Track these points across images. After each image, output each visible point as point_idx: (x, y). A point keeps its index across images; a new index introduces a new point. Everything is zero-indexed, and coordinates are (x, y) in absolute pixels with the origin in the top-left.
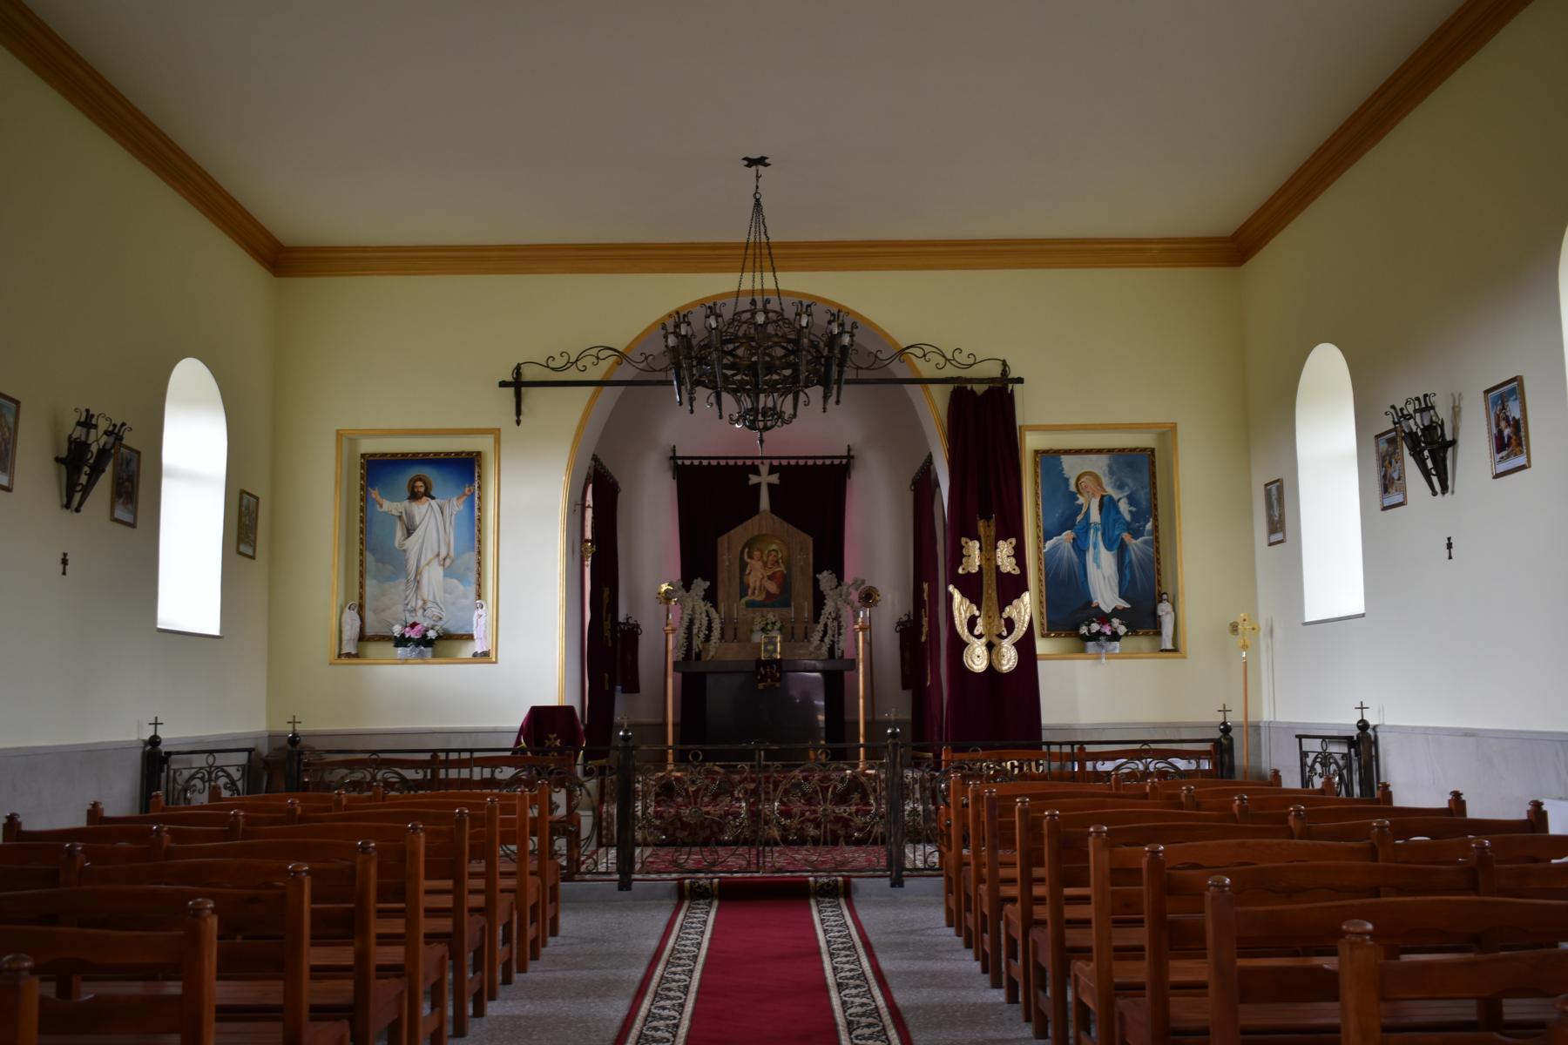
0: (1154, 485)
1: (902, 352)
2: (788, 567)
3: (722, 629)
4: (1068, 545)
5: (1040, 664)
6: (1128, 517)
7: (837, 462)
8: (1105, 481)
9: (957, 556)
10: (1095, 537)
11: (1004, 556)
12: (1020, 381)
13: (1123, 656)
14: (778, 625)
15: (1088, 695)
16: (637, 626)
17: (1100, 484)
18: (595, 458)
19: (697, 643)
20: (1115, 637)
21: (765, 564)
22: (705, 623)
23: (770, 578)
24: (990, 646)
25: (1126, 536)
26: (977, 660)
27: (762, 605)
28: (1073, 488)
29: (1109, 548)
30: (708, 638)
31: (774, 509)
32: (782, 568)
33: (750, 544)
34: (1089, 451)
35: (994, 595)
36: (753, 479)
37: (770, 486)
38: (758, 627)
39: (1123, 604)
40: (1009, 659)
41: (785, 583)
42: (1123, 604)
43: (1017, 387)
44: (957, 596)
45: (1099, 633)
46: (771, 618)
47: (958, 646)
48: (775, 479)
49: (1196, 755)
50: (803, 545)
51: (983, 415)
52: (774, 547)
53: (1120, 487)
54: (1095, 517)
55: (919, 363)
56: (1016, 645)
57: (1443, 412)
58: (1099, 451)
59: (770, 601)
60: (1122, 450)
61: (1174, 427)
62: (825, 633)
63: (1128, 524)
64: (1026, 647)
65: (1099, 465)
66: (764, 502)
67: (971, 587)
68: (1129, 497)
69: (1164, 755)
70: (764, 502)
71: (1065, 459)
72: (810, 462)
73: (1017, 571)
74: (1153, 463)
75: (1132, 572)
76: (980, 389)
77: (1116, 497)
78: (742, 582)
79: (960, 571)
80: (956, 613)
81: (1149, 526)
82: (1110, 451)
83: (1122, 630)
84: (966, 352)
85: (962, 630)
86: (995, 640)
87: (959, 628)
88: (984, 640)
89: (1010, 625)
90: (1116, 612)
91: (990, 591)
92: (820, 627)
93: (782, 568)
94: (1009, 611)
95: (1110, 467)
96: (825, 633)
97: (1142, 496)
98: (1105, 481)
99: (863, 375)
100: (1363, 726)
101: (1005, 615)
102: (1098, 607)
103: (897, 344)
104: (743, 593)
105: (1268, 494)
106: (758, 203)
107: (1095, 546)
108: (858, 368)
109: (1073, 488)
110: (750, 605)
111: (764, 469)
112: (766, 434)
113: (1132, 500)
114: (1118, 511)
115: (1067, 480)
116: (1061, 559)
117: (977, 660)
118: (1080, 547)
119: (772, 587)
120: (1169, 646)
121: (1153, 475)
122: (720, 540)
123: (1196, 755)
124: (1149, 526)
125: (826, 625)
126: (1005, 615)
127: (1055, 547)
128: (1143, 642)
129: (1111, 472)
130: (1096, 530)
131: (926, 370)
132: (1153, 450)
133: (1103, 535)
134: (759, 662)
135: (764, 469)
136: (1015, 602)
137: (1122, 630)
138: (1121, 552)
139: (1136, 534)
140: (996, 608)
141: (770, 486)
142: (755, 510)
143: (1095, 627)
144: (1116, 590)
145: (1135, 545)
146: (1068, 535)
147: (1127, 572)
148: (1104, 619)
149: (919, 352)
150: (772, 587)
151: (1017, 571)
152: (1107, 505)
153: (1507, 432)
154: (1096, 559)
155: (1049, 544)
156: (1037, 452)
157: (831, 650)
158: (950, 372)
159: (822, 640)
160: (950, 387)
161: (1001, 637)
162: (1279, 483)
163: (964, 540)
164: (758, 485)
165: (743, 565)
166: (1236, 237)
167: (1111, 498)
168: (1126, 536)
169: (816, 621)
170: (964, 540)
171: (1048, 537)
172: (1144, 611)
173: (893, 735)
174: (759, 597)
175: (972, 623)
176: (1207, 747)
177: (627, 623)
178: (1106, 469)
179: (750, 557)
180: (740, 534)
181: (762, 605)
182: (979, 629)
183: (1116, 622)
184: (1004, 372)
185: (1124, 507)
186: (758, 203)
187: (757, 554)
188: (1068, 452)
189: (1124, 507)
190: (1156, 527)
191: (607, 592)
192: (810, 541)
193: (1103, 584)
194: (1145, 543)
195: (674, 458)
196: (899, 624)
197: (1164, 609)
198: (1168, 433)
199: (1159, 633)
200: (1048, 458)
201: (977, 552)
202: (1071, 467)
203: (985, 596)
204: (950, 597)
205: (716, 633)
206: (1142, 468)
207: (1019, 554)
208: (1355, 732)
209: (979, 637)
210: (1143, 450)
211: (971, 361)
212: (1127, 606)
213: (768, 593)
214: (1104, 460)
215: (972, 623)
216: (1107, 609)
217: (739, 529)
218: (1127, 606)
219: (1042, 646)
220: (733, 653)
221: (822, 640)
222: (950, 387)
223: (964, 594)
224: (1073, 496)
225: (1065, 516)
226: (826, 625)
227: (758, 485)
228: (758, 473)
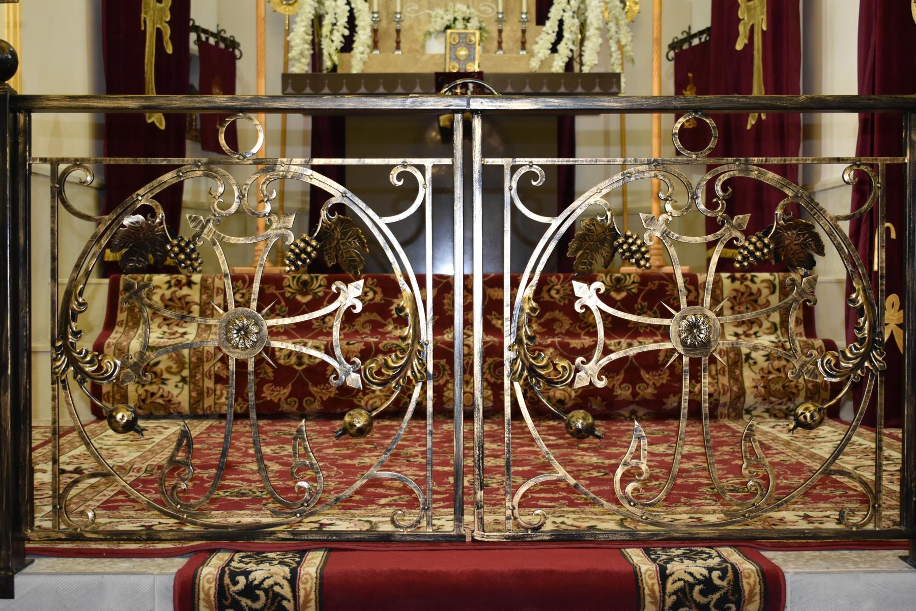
3: (375, 31)
16: (233, 44)
19: (331, 46)
22: (343, 20)
30: (348, 45)
38: (439, 25)
62: (560, 36)
92: (551, 26)
96: (560, 36)
125: (561, 23)
157: (569, 66)
159: (554, 50)
169: (542, 18)
196: (672, 47)
205: (363, 37)
221: (554, 50)
226: (561, 23)
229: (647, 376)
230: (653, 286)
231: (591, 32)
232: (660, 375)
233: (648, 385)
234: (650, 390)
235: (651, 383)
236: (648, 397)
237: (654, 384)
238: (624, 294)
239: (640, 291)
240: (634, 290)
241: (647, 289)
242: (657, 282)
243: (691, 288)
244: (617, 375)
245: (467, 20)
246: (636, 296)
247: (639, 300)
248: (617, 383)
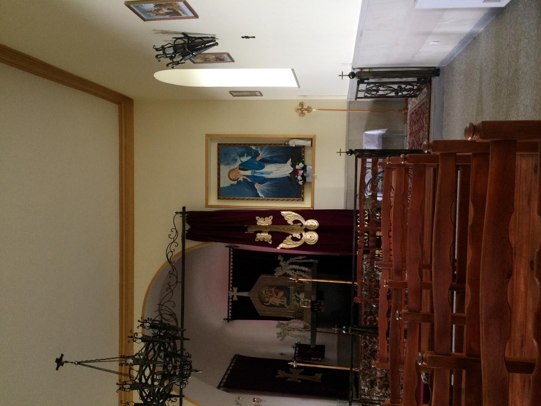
0: (235, 145)
1: (169, 261)
2: (272, 286)
4: (261, 186)
5: (315, 209)
6: (249, 158)
7: (232, 253)
8: (232, 167)
9: (263, 243)
10: (258, 173)
11: (265, 222)
12: (184, 208)
13: (313, 165)
14: (297, 294)
15: (331, 186)
16: (297, 344)
17: (234, 170)
18: (219, 387)
20: (304, 168)
21: (271, 296)
23: (277, 294)
24: (307, 230)
25: (258, 159)
26: (312, 237)
27: (288, 299)
28: (235, 182)
29: (263, 167)
31: (248, 290)
32: (273, 289)
33: (262, 302)
34: (219, 174)
35: (282, 226)
36: (235, 298)
37: (238, 291)
38: (298, 304)
39: (289, 162)
40: (313, 223)
41: (280, 288)
42: (289, 162)
43: (187, 210)
44: (282, 245)
45: (303, 176)
46: (293, 298)
47: (305, 246)
48: (235, 289)
49: (364, 169)
50: (264, 279)
51: (199, 225)
52: (264, 292)
53: (235, 160)
54: (249, 173)
55: (174, 253)
56: (306, 220)
57: (169, 39)
58: (219, 169)
59: (287, 295)
60: (219, 159)
61: (206, 135)
63: (252, 158)
64: (307, 214)
65: (225, 170)
66: (245, 294)
67: (278, 238)
68: (240, 157)
69: (363, 185)
70: (245, 294)
71: (222, 185)
72: (232, 264)
73: (271, 217)
74: (225, 144)
75: (275, 157)
76: (188, 227)
77: (240, 163)
78: (278, 307)
79: (271, 243)
80: (290, 247)
81: (254, 148)
82: (219, 165)
83: (301, 165)
84: (170, 233)
85: (299, 243)
86: (303, 228)
87: (297, 246)
88: (303, 234)
89: (296, 222)
90: (293, 165)
91: (281, 228)
93: (273, 289)
95: (226, 165)
97: (240, 150)
98: (232, 167)
99: (180, 280)
100: (352, 75)
101: (292, 224)
102: (290, 174)
103: (166, 263)
104: (283, 306)
105: (236, 96)
106: (79, 363)
107: (262, 173)
108: (177, 282)
109: (235, 182)
110: (288, 304)
111: (231, 294)
112: (194, 368)
113: (242, 155)
114: (246, 162)
115: (232, 185)
116: (267, 190)
117: (312, 237)
118: (263, 181)
119: (281, 294)
120: (309, 143)
121: (230, 145)
122: (260, 315)
123: (364, 169)
124: (254, 148)
127: (263, 192)
128: (308, 154)
129: (228, 164)
130: (255, 173)
131: (179, 249)
132: (219, 144)
133: (257, 169)
134: (312, 309)
135: (231, 294)
137: (301, 165)
138: (265, 161)
140: (288, 227)
141: (238, 291)
142: (247, 299)
143: (299, 178)
144: (283, 165)
145: (262, 155)
146: (257, 186)
147: (275, 159)
148: (295, 172)
149: (170, 255)
150: (281, 294)
151: (271, 217)
152: (244, 167)
153: (165, 10)
154: (268, 173)
155: (261, 195)
156: (218, 198)
158: (179, 240)
160: (186, 241)
161: (302, 225)
162: (231, 92)
163: (256, 240)
164: (238, 296)
165: (271, 305)
166: (119, 103)
167: (240, 165)
168: (258, 159)
170: (256, 240)
171: (257, 195)
172: (293, 153)
173: (346, 330)
174: (285, 300)
175: (295, 239)
176: (359, 160)
177: (296, 347)
178: (227, 166)
179: (268, 302)
180: (258, 306)
181: (288, 299)
182: (297, 235)
183: (297, 167)
184: (180, 213)
185: (245, 159)
186: (79, 363)
187: (266, 300)
188: (219, 184)
189: (245, 159)
190: (254, 145)
191: (281, 374)
192: (262, 276)
193: (281, 170)
194: (261, 150)
195: (228, 320)
197: (292, 143)
198: (209, 137)
199: (304, 146)
200: (222, 193)
201: (262, 234)
202: (226, 183)
203: (283, 231)
204: (282, 248)
206: (227, 150)
207: (264, 214)
208: (356, 80)
209: (301, 235)
210: (219, 149)
211: (175, 231)
212: (290, 160)
213: (283, 296)
214: (222, 167)
215: (295, 239)
216: (292, 169)
217: (256, 306)
218: (290, 160)
219: (306, 204)
220: (308, 316)
222: (186, 241)
223: (282, 242)
224: (239, 182)
225: (247, 188)
227: (238, 296)
228: (233, 296)
231: (300, 268)
245: (296, 297)
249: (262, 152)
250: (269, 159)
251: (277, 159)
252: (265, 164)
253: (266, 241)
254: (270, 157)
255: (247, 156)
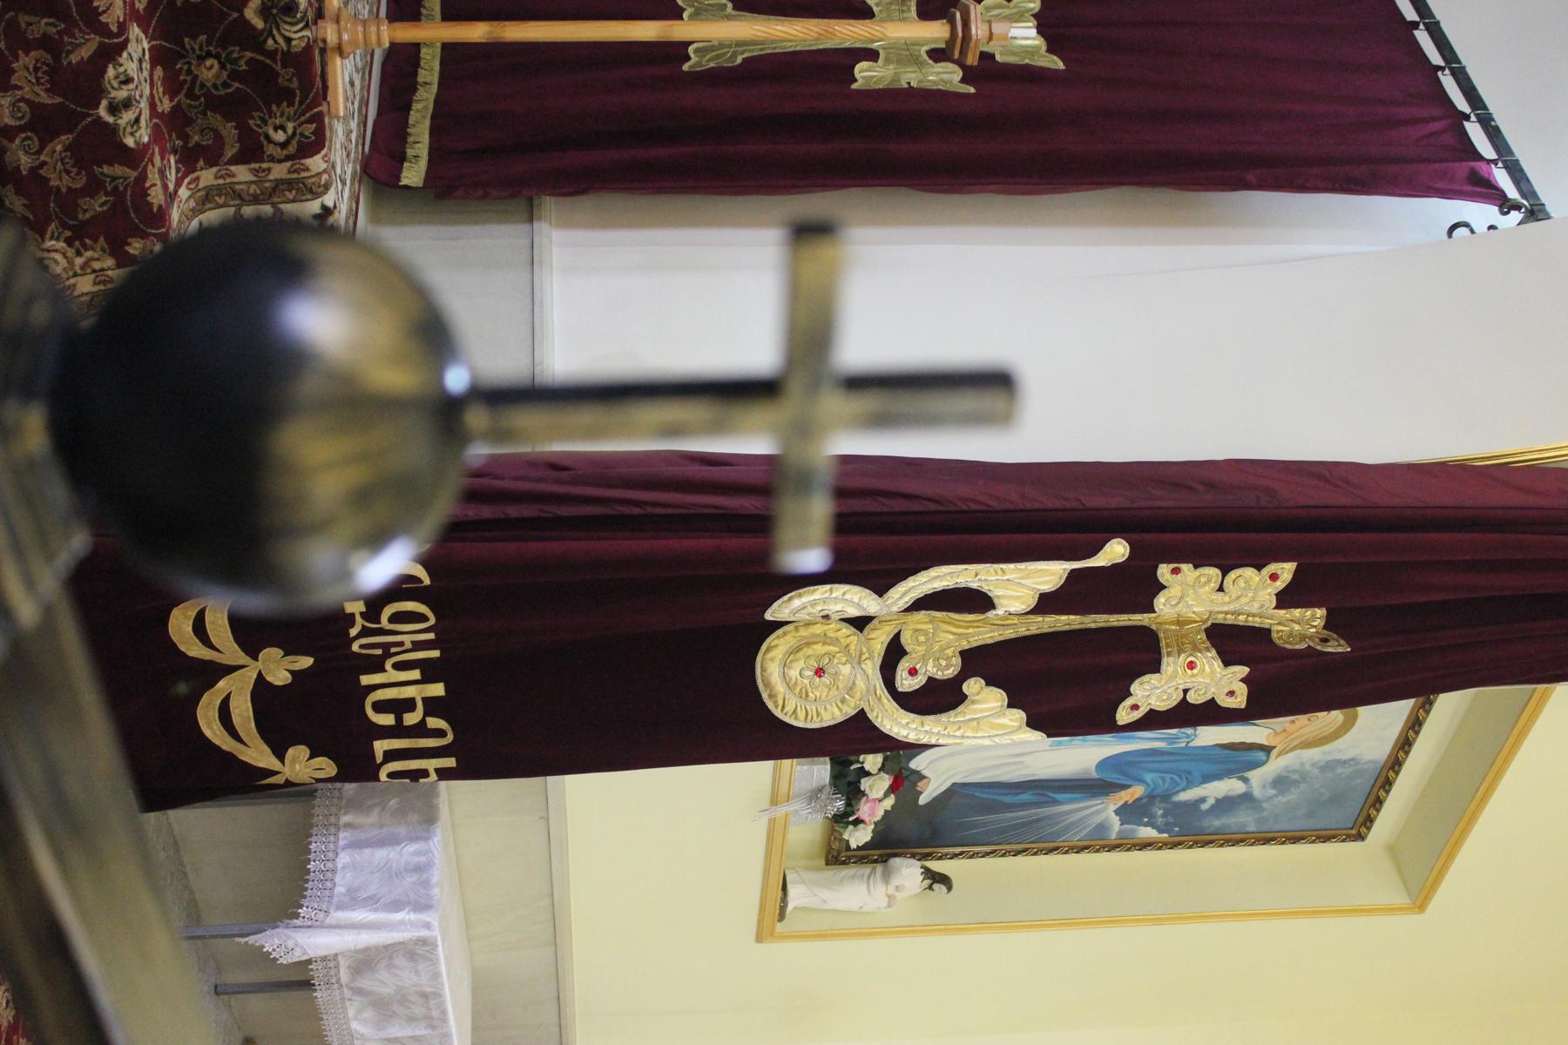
6: (1184, 796)
53: (1281, 783)
63: (1166, 797)
68: (1247, 797)
77: (1255, 776)
89: (938, 698)
94: (985, 699)
124: (1147, 833)
126: (973, 686)
136: (1019, 716)
139: (1129, 813)
151: (1124, 715)
170: (1286, 570)
210: (1369, 821)
212: (923, 800)
218: (923, 800)
229: (59, 148)
230: (287, 77)
232: (68, 172)
233: (39, 152)
234: (25, 161)
235: (42, 158)
236: (8, 157)
237: (44, 163)
238: (259, 23)
239: (272, 54)
240: (270, 42)
241: (278, 67)
242: (295, 84)
243: (292, 149)
244: (47, 90)
246: (259, 47)
247: (248, 54)
248: (26, 92)
249: (1098, 819)
250: (1059, 796)
251: (1008, 799)
252: (1095, 775)
253: (1214, 572)
254: (1056, 802)
255: (1203, 800)
